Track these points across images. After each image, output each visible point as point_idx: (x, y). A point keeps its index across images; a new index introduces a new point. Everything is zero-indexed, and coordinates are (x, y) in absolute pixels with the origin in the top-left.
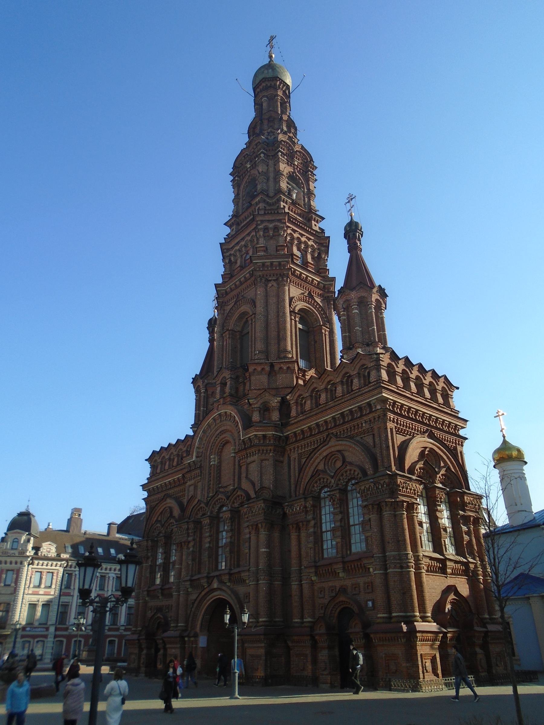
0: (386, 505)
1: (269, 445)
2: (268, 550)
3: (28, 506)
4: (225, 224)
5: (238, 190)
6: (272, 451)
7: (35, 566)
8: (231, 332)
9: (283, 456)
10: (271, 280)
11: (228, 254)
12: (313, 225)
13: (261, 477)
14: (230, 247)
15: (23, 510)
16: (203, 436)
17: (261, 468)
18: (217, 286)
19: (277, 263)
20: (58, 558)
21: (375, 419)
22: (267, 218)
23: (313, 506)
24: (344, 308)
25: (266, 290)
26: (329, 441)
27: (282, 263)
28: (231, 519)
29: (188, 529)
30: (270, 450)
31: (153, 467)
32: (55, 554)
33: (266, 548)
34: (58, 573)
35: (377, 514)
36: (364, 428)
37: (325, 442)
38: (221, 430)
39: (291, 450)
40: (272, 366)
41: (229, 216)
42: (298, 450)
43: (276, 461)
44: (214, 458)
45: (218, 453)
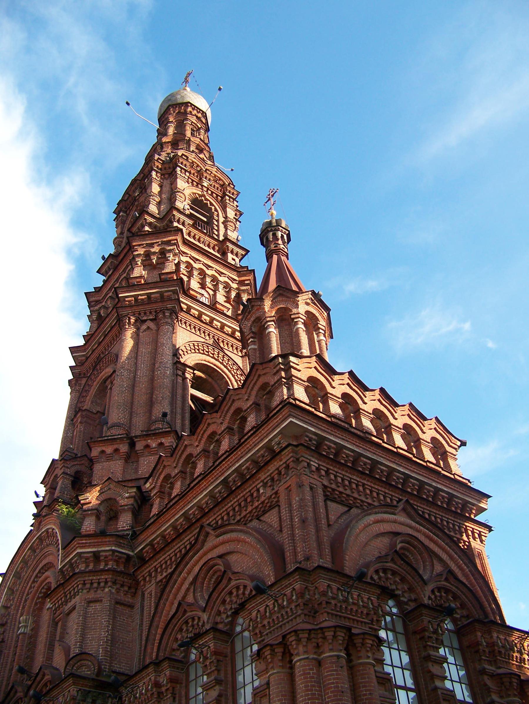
0: (299, 640)
5: (122, 228)
6: (109, 584)
8: (84, 413)
9: (134, 595)
10: (145, 321)
11: (96, 308)
13: (83, 636)
14: (101, 298)
16: (14, 583)
17: (85, 618)
18: (73, 350)
19: (158, 295)
21: (280, 473)
23: (172, 680)
24: (253, 333)
26: (204, 541)
27: (166, 294)
30: (106, 582)
35: (283, 667)
36: (263, 498)
38: (41, 566)
39: (145, 579)
40: (132, 445)
42: (156, 577)
43: (117, 603)
44: (26, 621)
45: (34, 611)
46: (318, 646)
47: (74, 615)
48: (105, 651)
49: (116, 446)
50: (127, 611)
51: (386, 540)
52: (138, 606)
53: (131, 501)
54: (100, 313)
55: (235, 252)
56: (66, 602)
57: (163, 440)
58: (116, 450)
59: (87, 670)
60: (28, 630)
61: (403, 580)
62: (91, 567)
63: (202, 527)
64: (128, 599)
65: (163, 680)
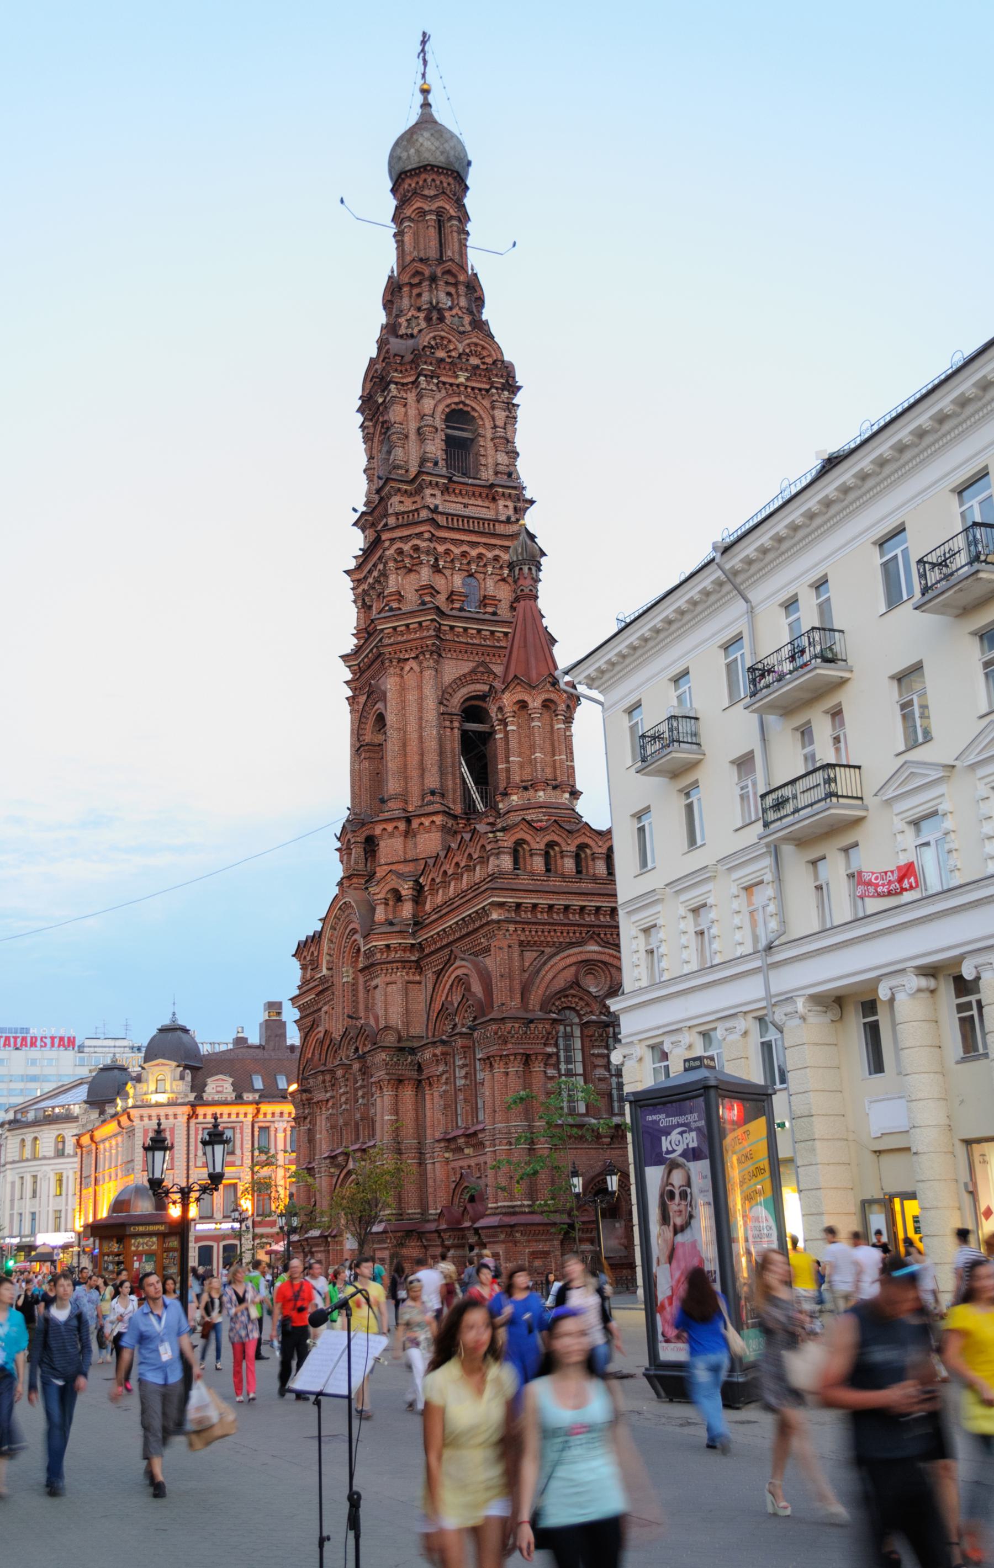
1: (393, 962)
2: (393, 1118)
3: (174, 1014)
4: (355, 524)
7: (201, 1119)
10: (408, 659)
11: (360, 590)
12: (501, 507)
13: (386, 1010)
14: (362, 576)
15: (166, 1021)
17: (386, 996)
20: (239, 1100)
22: (398, 534)
25: (402, 677)
28: (360, 1070)
29: (324, 1082)
31: (304, 968)
32: (234, 1095)
33: (391, 1114)
34: (241, 1129)
37: (448, 963)
40: (408, 821)
41: (355, 510)
44: (347, 972)
46: (506, 1063)
47: (378, 991)
48: (403, 1022)
49: (395, 824)
50: (417, 986)
51: (573, 969)
52: (423, 983)
53: (410, 892)
54: (364, 600)
55: (507, 495)
56: (372, 979)
57: (434, 818)
58: (396, 827)
59: (391, 1039)
60: (350, 979)
61: (581, 999)
62: (385, 956)
63: (451, 951)
64: (417, 978)
65: (438, 1052)
